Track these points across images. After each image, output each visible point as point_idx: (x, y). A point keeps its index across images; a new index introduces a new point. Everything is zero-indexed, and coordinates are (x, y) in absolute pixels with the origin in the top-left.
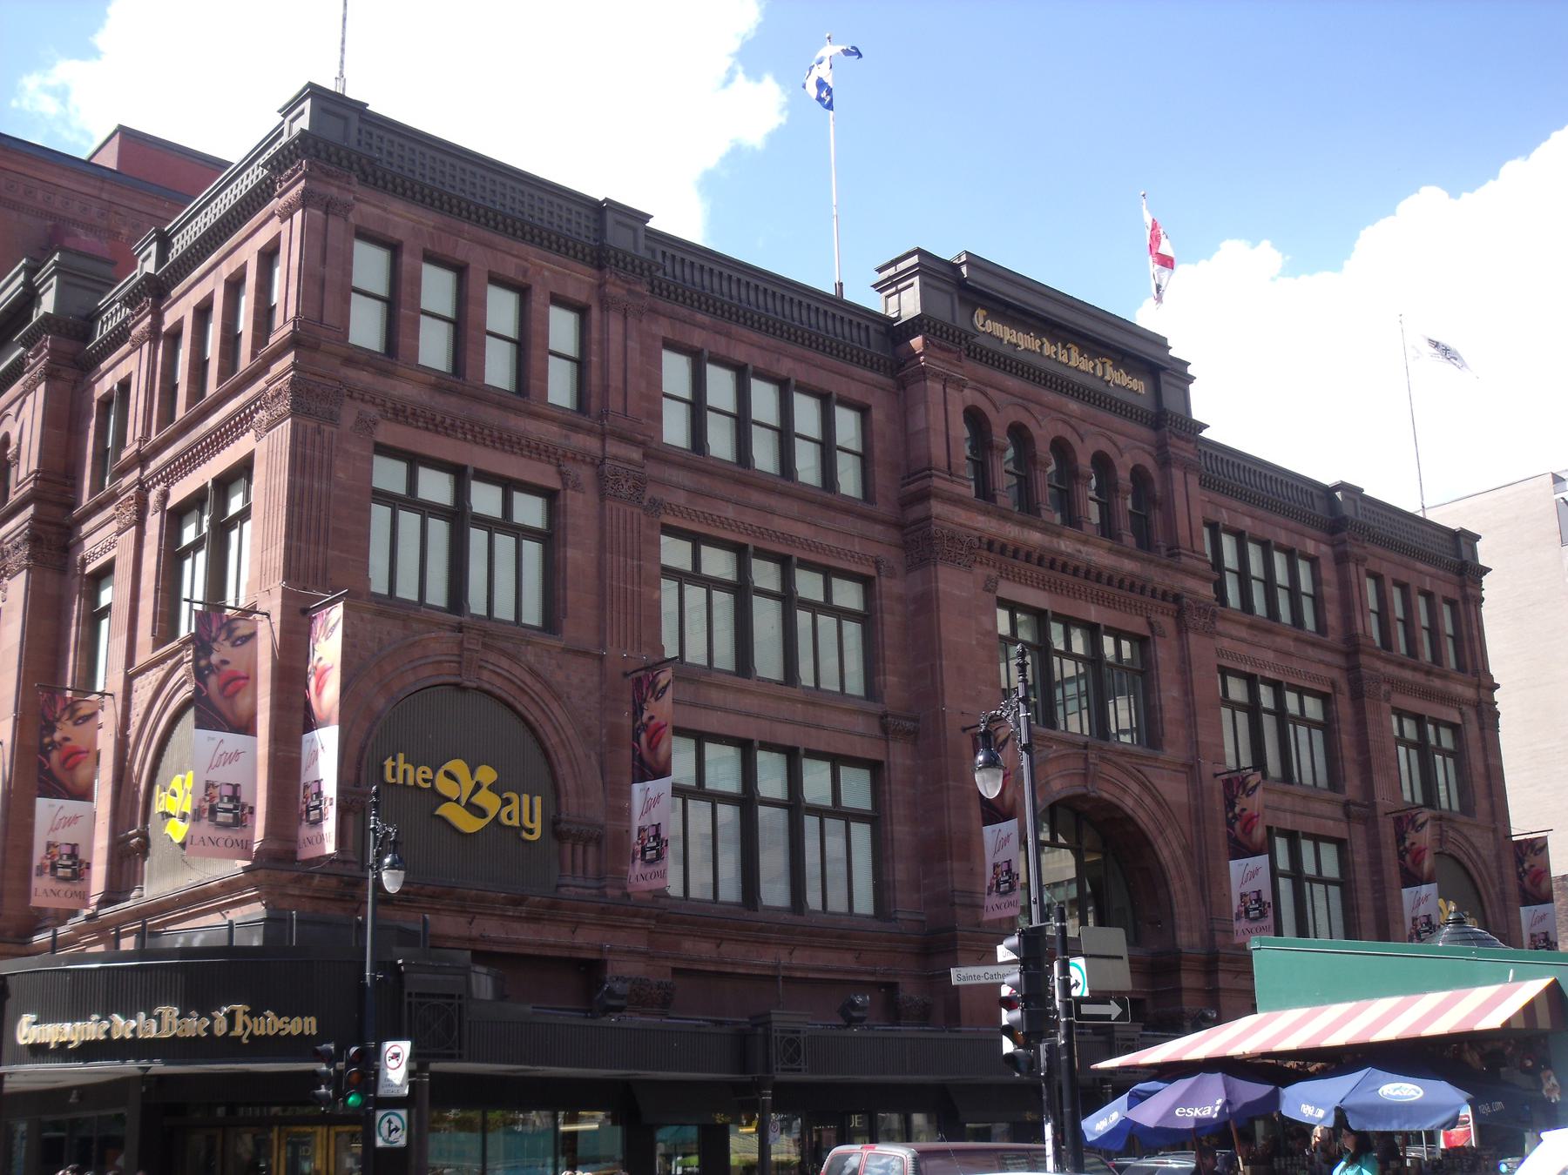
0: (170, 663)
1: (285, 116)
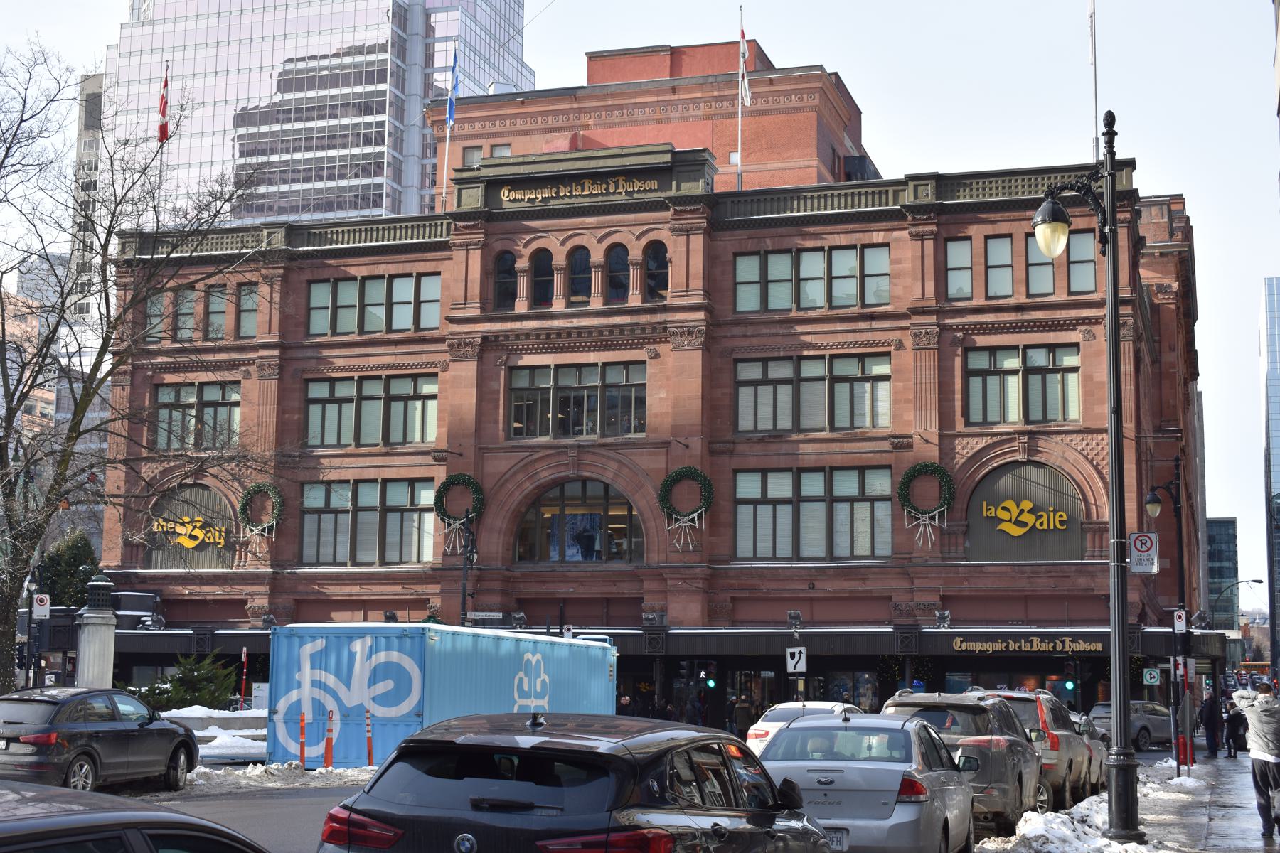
0: (999, 438)
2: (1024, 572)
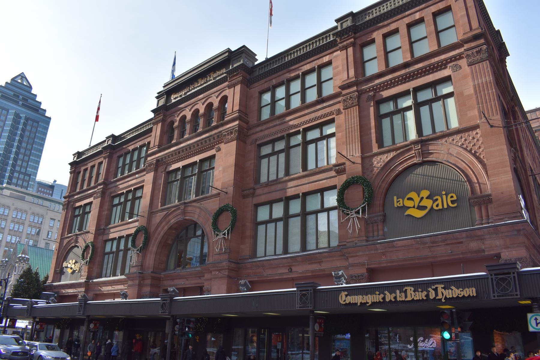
2: (425, 243)
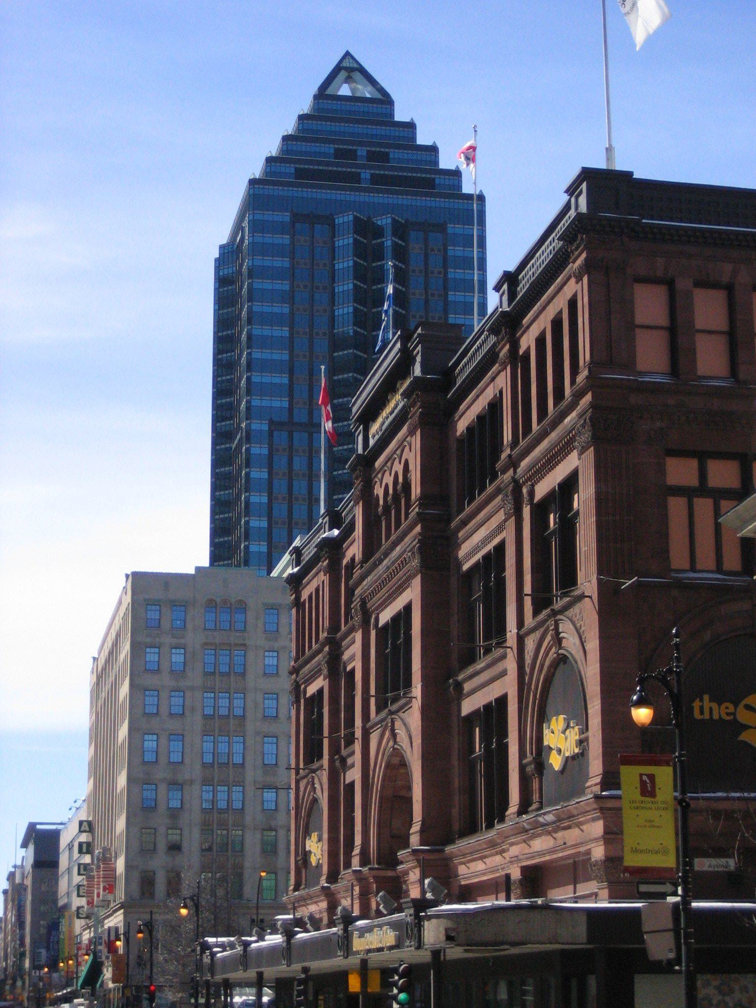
0: (542, 630)
1: (571, 195)
